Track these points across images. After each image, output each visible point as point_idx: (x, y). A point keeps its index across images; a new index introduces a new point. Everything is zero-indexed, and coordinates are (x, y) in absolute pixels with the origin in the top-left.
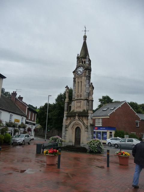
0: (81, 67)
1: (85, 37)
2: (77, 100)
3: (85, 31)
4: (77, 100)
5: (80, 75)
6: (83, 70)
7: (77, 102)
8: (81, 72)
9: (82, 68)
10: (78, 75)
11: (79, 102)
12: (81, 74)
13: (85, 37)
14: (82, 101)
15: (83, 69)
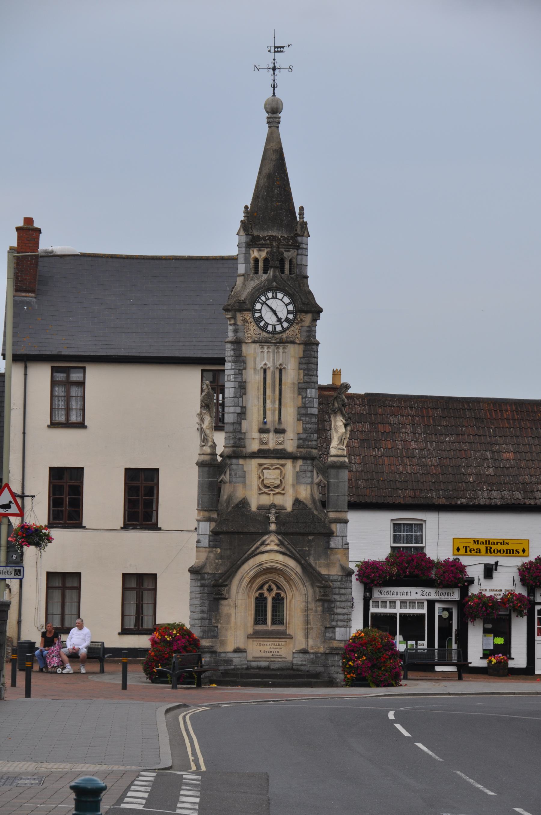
0: (280, 295)
1: (274, 111)
2: (262, 454)
3: (274, 69)
4: (262, 454)
5: (274, 332)
6: (289, 312)
7: (260, 465)
8: (279, 320)
9: (287, 300)
10: (264, 329)
11: (272, 465)
12: (279, 328)
13: (274, 111)
14: (289, 464)
15: (291, 308)
